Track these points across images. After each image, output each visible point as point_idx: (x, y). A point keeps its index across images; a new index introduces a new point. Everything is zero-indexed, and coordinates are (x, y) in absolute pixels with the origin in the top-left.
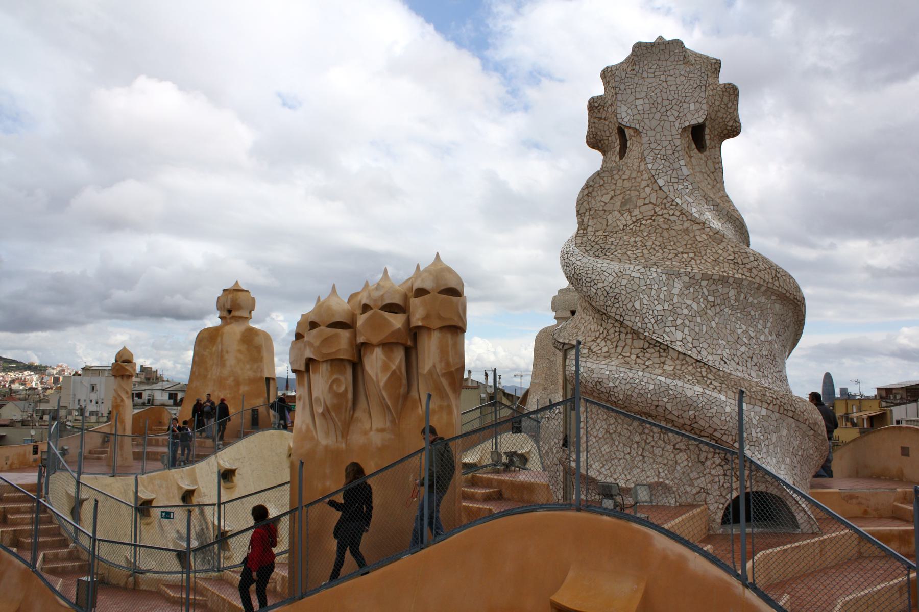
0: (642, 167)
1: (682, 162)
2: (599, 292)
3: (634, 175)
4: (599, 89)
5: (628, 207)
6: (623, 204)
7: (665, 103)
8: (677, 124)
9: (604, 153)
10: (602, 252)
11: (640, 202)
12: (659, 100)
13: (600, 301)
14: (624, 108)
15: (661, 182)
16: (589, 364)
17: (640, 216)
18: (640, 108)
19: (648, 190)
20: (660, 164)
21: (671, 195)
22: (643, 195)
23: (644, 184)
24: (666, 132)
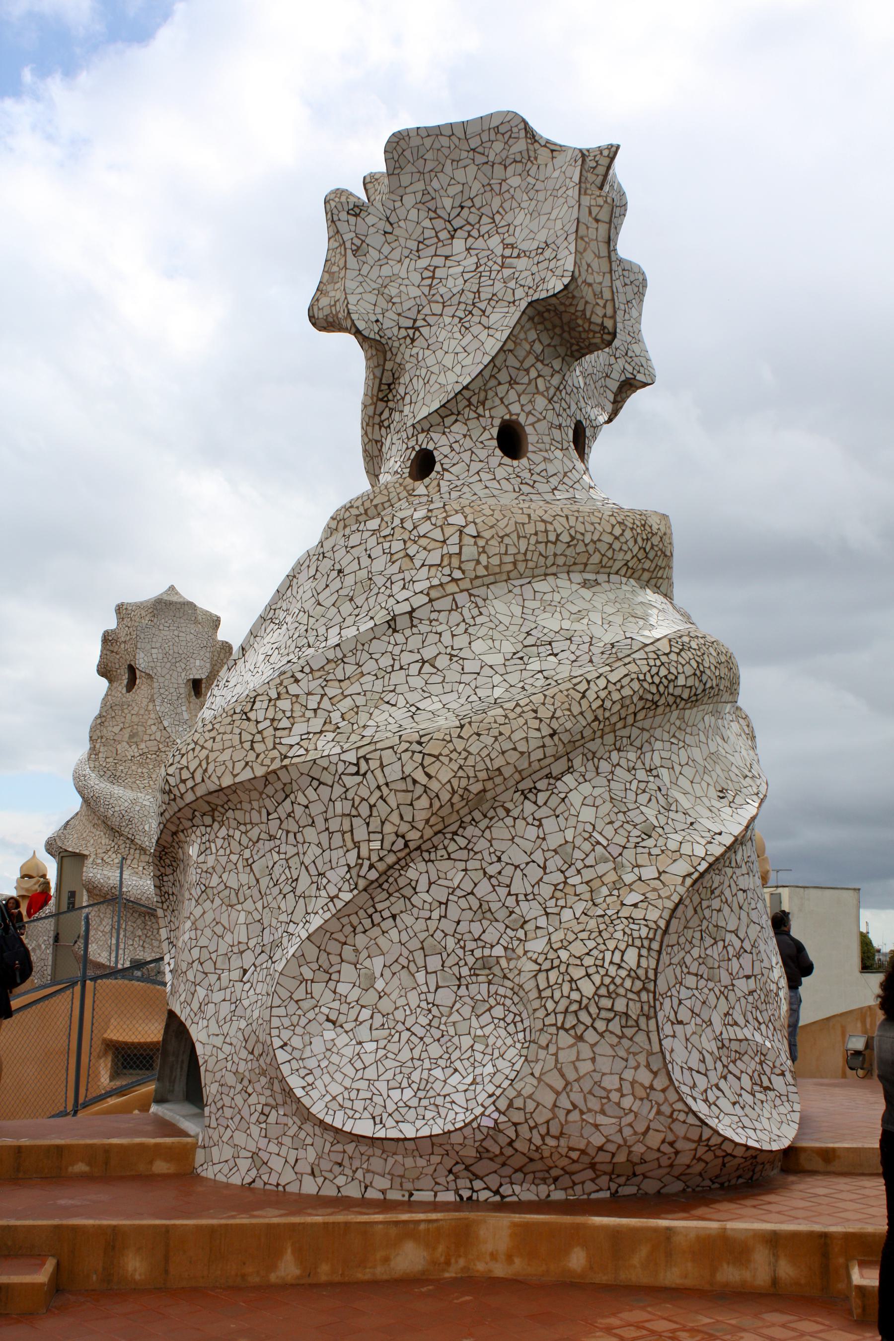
0: (151, 707)
1: (184, 708)
2: (116, 814)
3: (142, 712)
4: (112, 623)
5: (135, 740)
6: (131, 737)
7: (176, 655)
8: (183, 674)
9: (110, 681)
10: (114, 778)
11: (146, 738)
12: (171, 652)
13: (115, 821)
14: (142, 655)
15: (166, 723)
16: (105, 872)
17: (146, 750)
18: (154, 656)
19: (154, 728)
20: (166, 708)
21: (173, 735)
22: (149, 732)
23: (150, 722)
24: (173, 680)
